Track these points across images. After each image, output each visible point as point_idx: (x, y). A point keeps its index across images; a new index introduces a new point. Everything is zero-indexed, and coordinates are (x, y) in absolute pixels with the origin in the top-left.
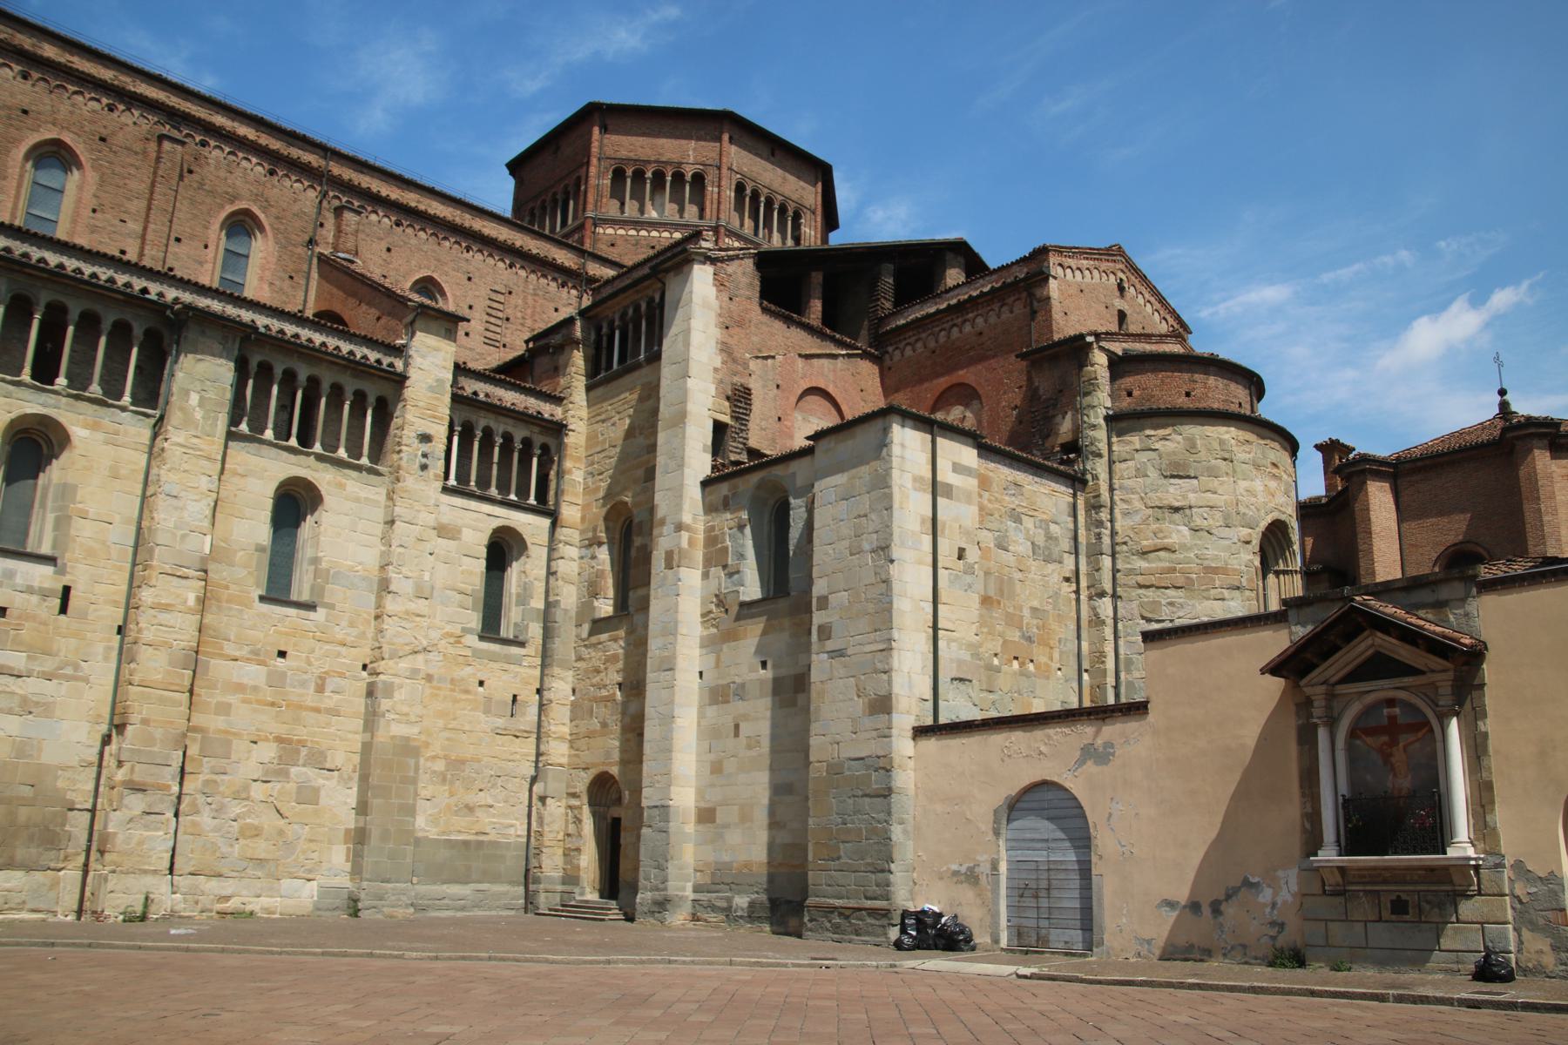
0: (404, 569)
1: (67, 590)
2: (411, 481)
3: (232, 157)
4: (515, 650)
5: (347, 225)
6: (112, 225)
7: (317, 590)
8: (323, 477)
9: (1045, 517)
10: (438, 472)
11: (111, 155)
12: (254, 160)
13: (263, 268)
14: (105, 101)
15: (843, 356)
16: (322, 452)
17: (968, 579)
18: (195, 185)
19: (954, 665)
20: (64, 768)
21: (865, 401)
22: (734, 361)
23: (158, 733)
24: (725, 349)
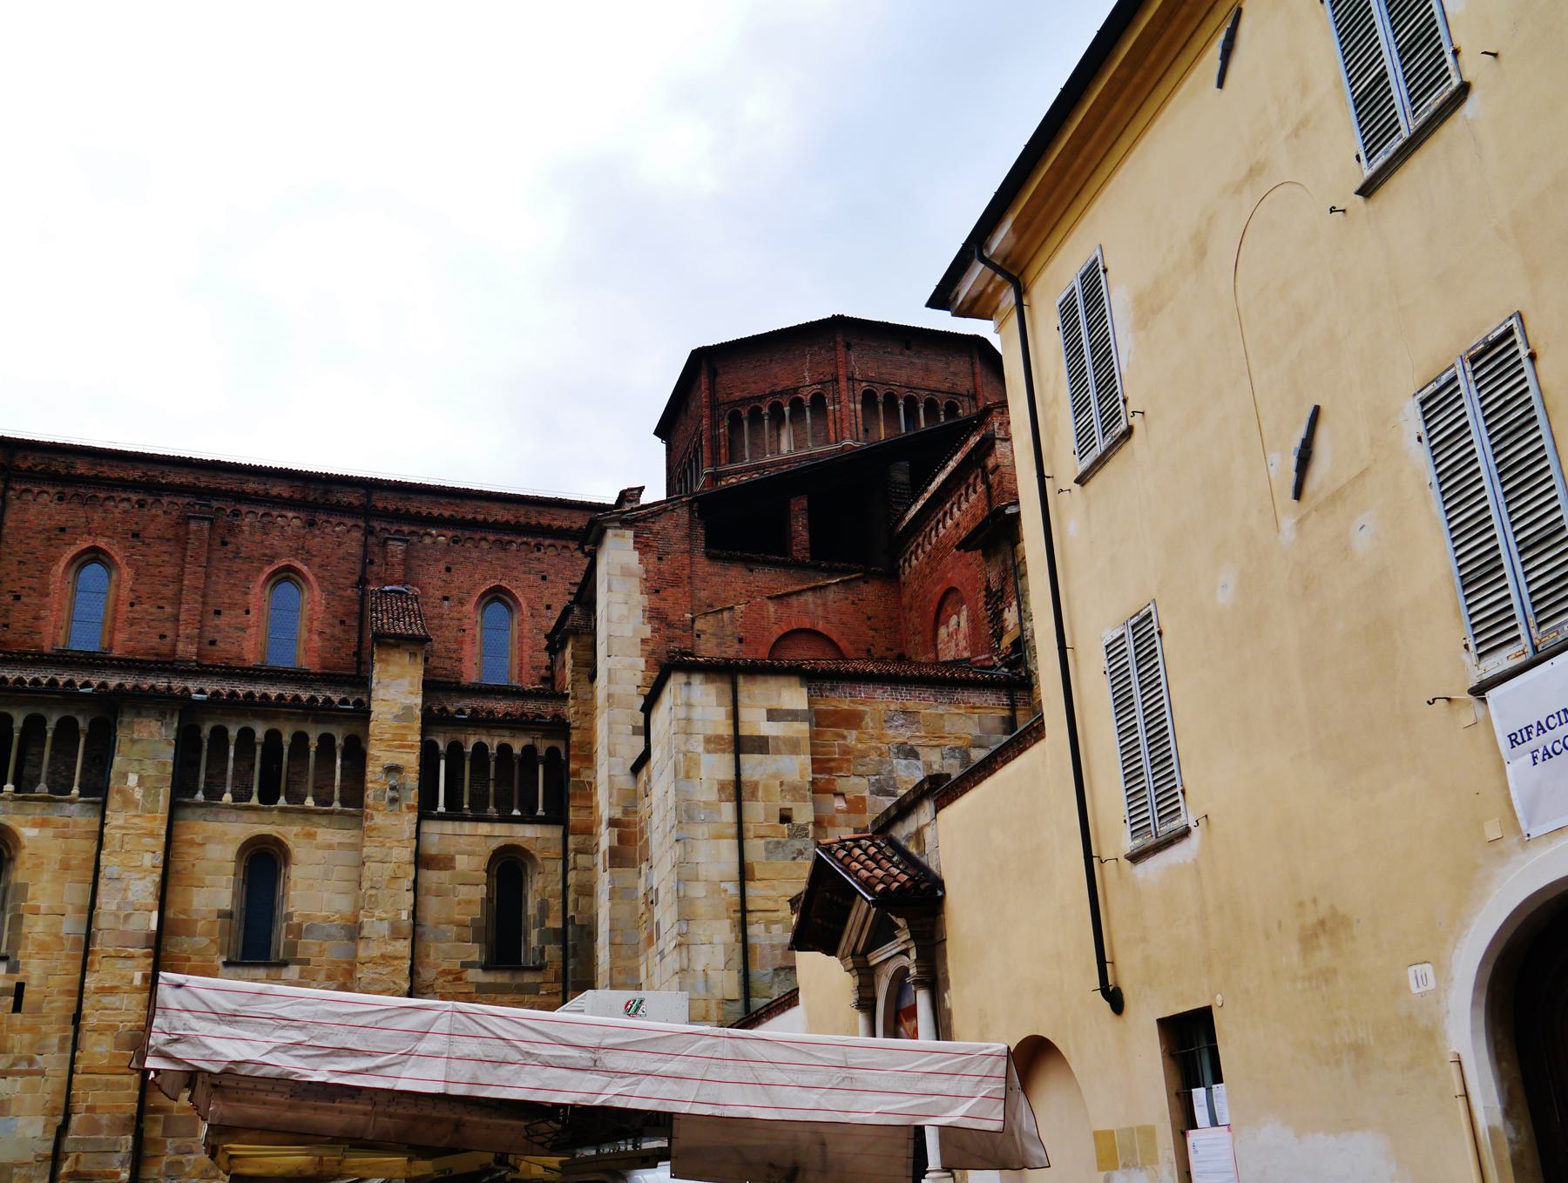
0: (377, 913)
1: (20, 987)
2: (379, 819)
3: (265, 519)
4: (528, 978)
5: (392, 557)
6: (151, 614)
7: (292, 948)
8: (289, 832)
9: (960, 743)
10: (412, 803)
11: (144, 548)
12: (290, 515)
13: (311, 620)
14: (134, 497)
15: (837, 583)
16: (286, 805)
17: (798, 844)
18: (231, 556)
19: (778, 952)
20: (21, 1165)
21: (876, 630)
22: (670, 625)
23: (104, 1119)
24: (656, 616)
